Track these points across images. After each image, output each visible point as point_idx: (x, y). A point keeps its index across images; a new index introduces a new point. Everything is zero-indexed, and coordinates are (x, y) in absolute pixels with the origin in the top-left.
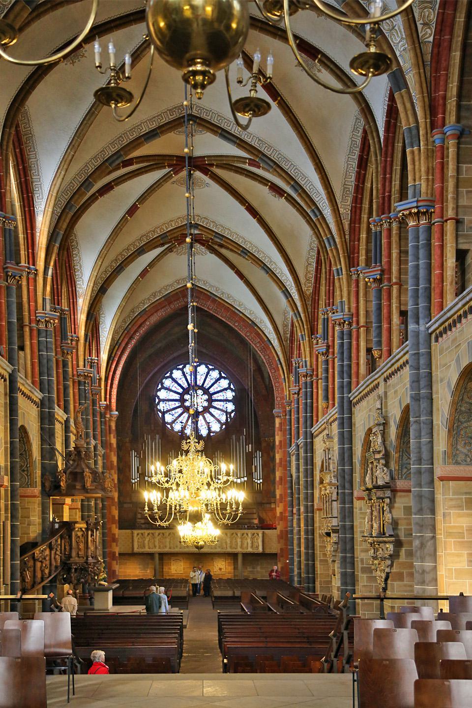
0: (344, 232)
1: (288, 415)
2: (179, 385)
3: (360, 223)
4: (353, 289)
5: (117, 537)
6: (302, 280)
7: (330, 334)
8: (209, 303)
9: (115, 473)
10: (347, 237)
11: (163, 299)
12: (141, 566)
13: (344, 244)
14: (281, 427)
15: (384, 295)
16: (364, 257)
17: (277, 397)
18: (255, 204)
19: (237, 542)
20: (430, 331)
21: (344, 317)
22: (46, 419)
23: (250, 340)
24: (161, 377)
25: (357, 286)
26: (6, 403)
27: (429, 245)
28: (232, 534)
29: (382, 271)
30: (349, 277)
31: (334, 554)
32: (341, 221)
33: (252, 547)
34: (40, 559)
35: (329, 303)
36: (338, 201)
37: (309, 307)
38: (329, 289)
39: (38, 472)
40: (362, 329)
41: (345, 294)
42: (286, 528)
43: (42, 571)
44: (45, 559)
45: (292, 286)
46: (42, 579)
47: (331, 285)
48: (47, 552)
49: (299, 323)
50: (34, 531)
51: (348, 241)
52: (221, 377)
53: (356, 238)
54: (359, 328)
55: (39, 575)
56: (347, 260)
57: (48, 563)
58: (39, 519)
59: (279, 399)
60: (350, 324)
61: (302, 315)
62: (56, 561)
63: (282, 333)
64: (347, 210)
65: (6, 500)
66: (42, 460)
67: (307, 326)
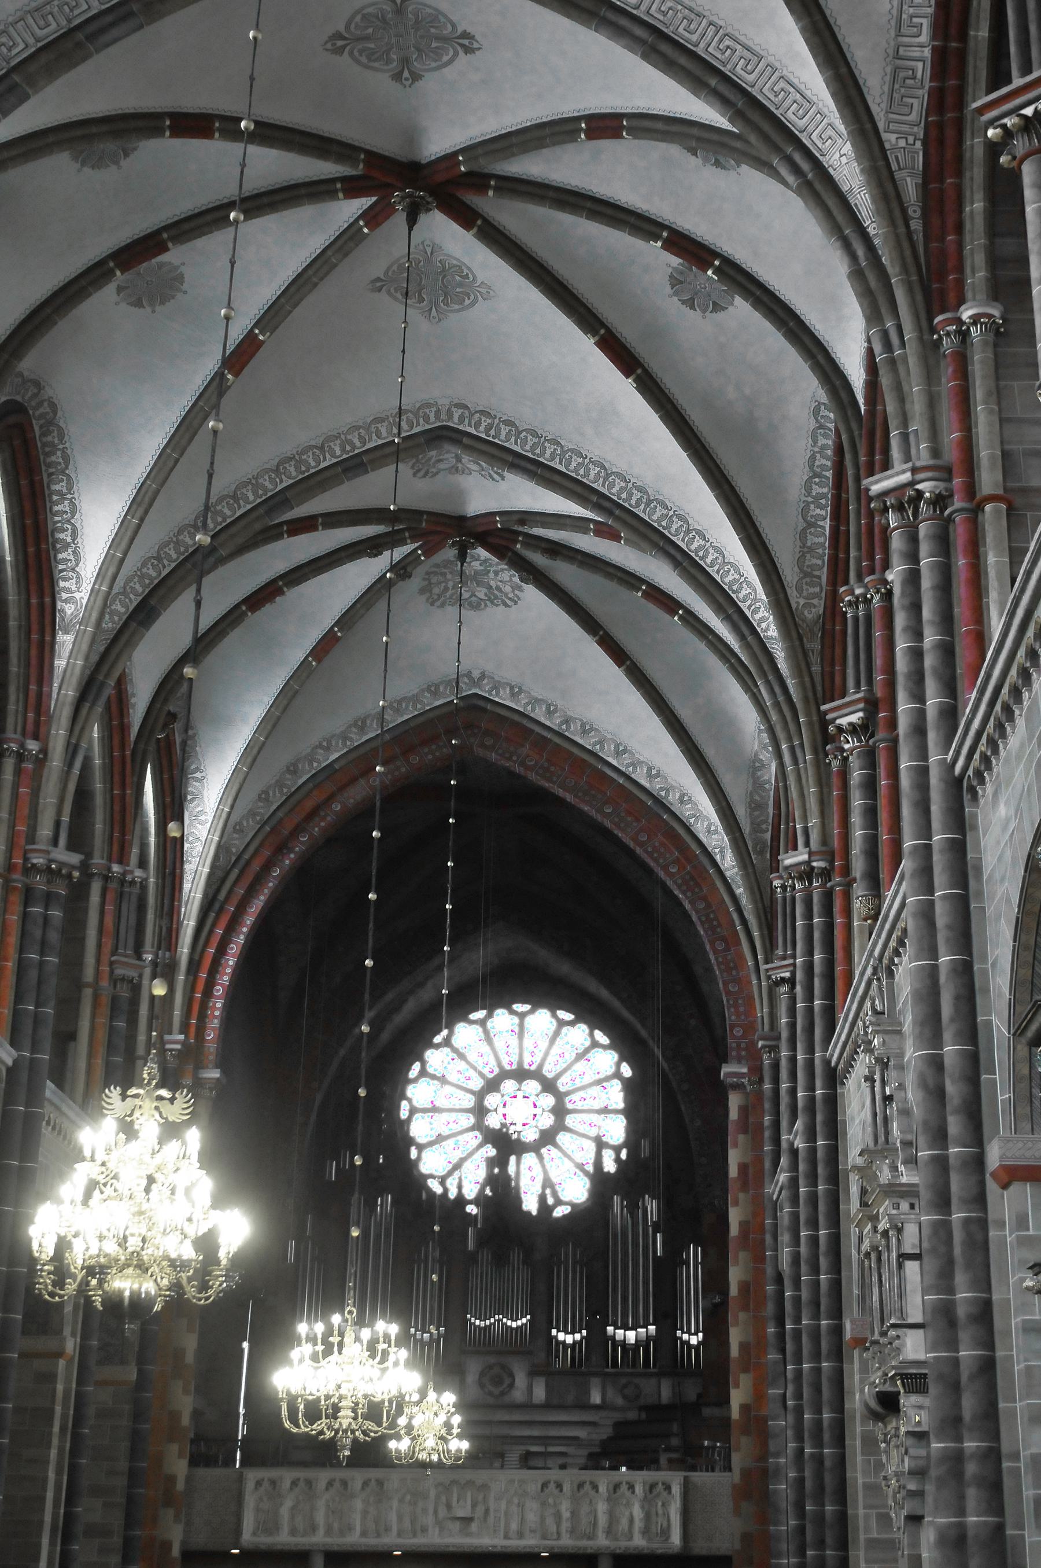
0: (904, 211)
3: (959, 173)
4: (948, 383)
8: (525, 750)
10: (916, 225)
13: (906, 245)
14: (747, 1117)
16: (981, 274)
17: (732, 1027)
18: (629, 334)
23: (650, 854)
25: (963, 372)
30: (930, 348)
31: (912, 1486)
32: (891, 173)
36: (875, 109)
37: (815, 659)
45: (756, 600)
49: (780, 711)
51: (919, 238)
53: (950, 221)
56: (919, 297)
59: (738, 1032)
61: (790, 683)
63: (746, 828)
64: (911, 140)
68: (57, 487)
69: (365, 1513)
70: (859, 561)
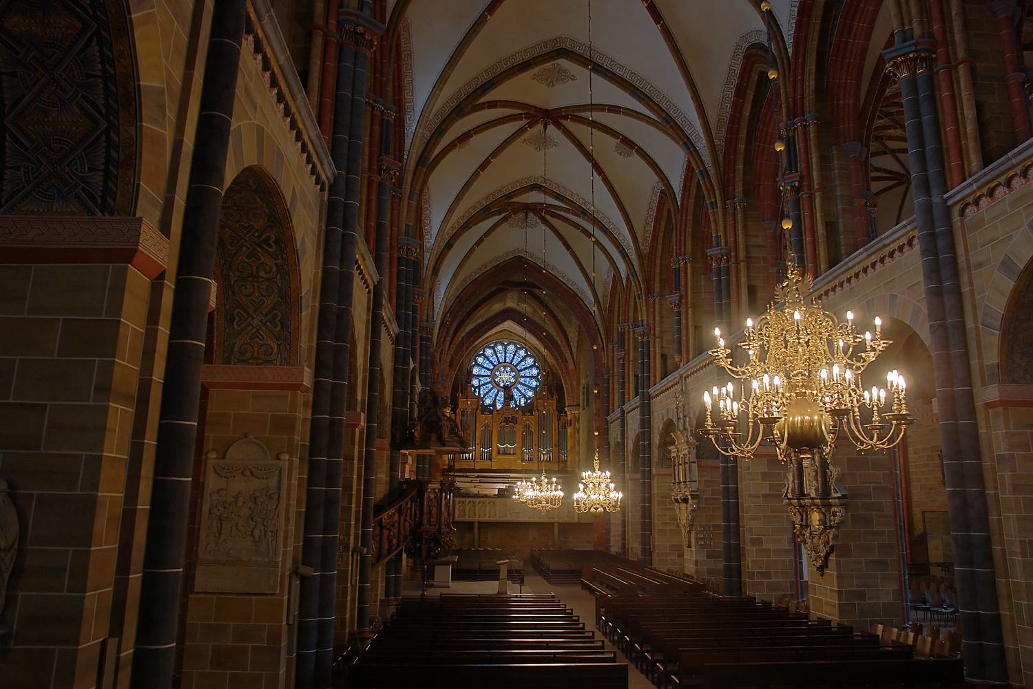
2: (491, 362)
6: (640, 239)
7: (683, 283)
10: (721, 169)
11: (493, 269)
15: (805, 204)
20: (949, 203)
21: (722, 251)
22: (400, 358)
26: (368, 321)
27: (932, 98)
29: (801, 179)
30: (725, 210)
34: (388, 527)
35: (680, 253)
36: (713, 132)
38: (680, 239)
39: (389, 420)
40: (742, 264)
41: (721, 228)
43: (390, 542)
44: (393, 526)
46: (389, 551)
47: (683, 234)
48: (396, 517)
50: (381, 490)
52: (527, 356)
54: (739, 263)
55: (386, 546)
57: (396, 531)
58: (386, 476)
60: (728, 261)
62: (405, 530)
65: (360, 446)
66: (393, 406)
67: (644, 284)
68: (426, 206)
69: (490, 510)
70: (676, 249)
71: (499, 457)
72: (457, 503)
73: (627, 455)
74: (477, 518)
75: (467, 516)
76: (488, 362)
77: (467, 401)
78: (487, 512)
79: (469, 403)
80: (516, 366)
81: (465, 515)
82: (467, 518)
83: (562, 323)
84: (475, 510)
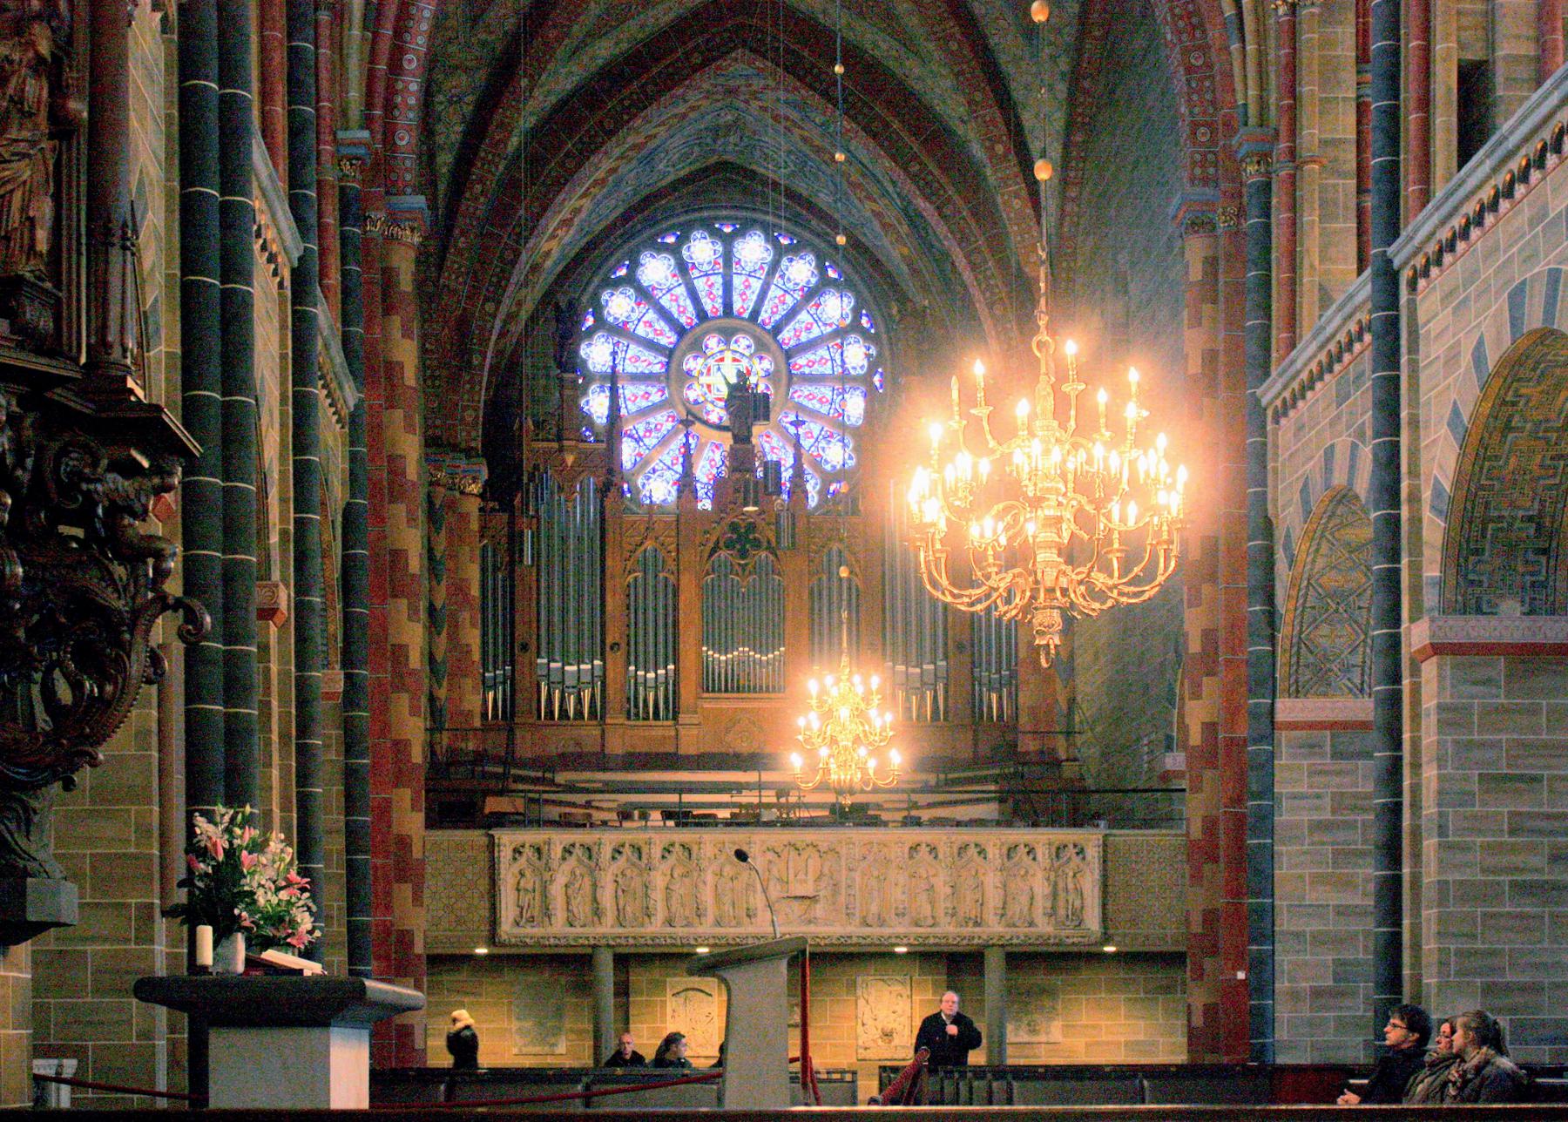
1: (1254, 211)
2: (664, 314)
5: (417, 853)
9: (411, 521)
12: (528, 1024)
19: (980, 886)
24: (596, 280)
28: (963, 849)
33: (1052, 913)
42: (1239, 800)
52: (824, 284)
71: (710, 704)
72: (505, 854)
73: (1416, 521)
74: (607, 928)
75: (560, 916)
76: (651, 316)
77: (561, 450)
78: (658, 896)
79: (570, 459)
80: (777, 329)
81: (547, 913)
82: (558, 930)
83: (993, 41)
84: (595, 885)
